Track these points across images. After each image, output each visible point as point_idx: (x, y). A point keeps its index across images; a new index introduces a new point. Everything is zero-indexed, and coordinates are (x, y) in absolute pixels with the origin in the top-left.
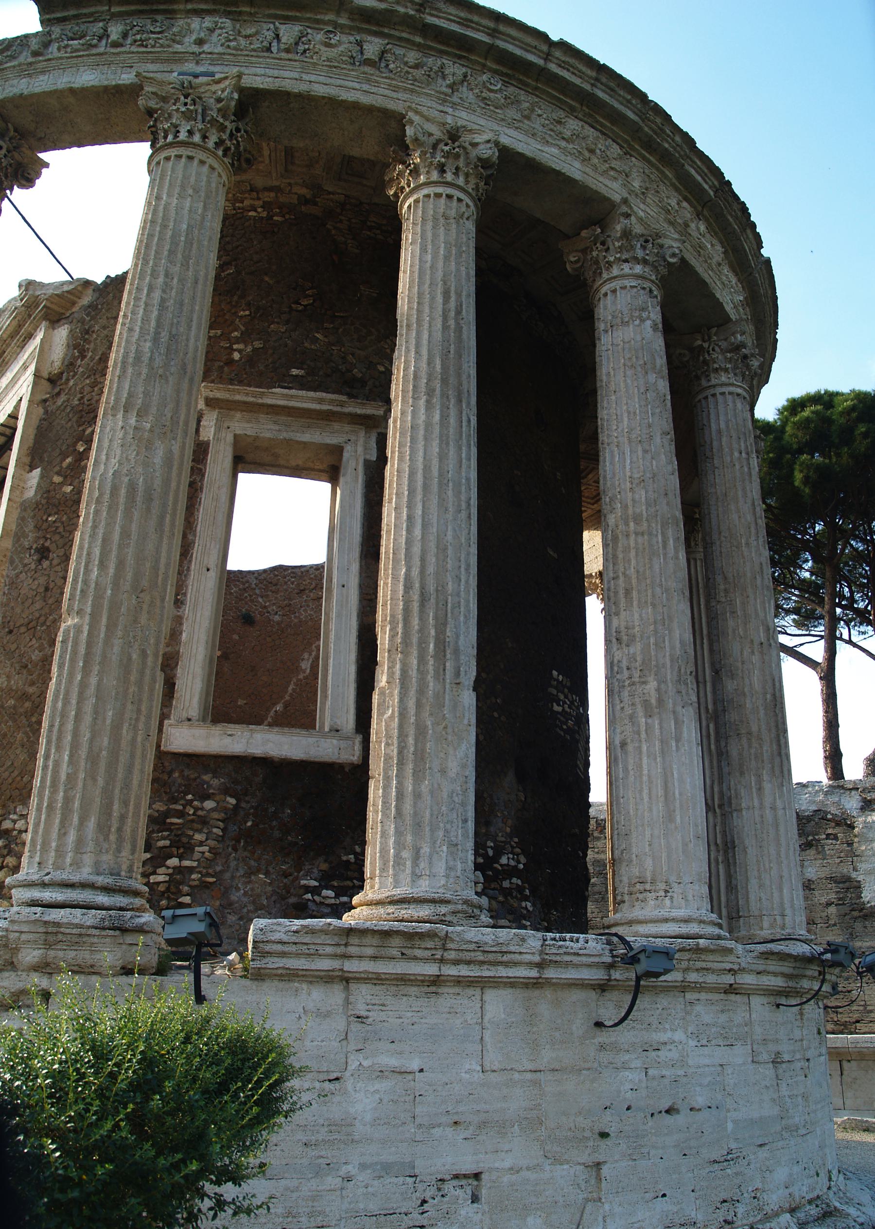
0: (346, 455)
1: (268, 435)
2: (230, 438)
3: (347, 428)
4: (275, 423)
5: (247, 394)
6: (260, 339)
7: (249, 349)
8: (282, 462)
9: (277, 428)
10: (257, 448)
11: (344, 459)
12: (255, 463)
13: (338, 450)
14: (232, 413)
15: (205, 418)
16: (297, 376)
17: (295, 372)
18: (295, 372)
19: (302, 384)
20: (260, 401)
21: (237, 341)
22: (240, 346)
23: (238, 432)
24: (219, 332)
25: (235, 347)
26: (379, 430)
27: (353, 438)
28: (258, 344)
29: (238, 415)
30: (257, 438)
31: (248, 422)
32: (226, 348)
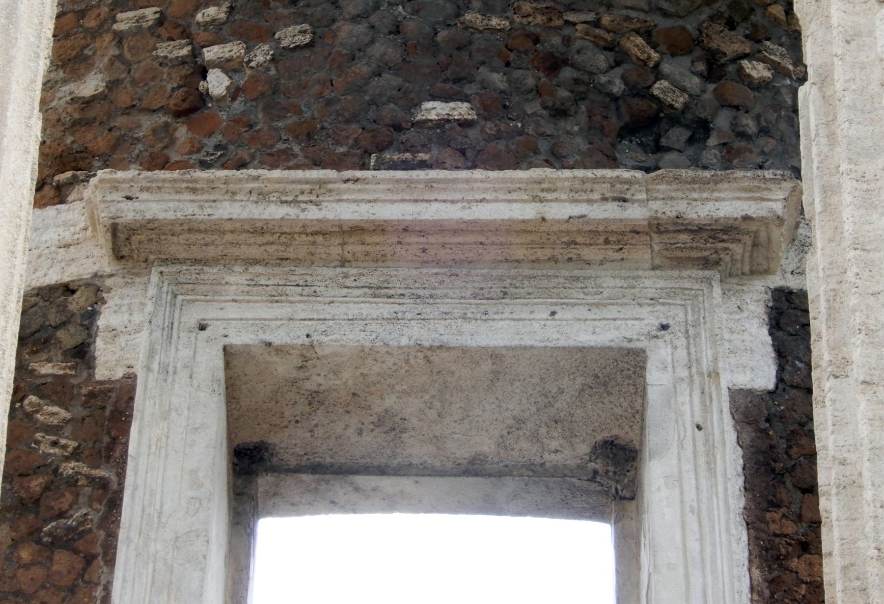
0: (657, 378)
1: (353, 337)
2: (211, 362)
3: (652, 283)
4: (377, 291)
5: (263, 196)
6: (303, 18)
7: (261, 54)
8: (417, 450)
9: (385, 309)
10: (315, 399)
11: (653, 394)
12: (317, 469)
13: (624, 370)
14: (212, 272)
15: (113, 300)
16: (442, 123)
17: (434, 110)
18: (434, 110)
19: (462, 148)
20: (313, 214)
21: (217, 33)
22: (232, 49)
23: (240, 338)
24: (150, 13)
25: (211, 53)
26: (776, 281)
27: (676, 315)
28: (292, 35)
29: (237, 278)
30: (307, 356)
31: (274, 299)
32: (183, 61)
